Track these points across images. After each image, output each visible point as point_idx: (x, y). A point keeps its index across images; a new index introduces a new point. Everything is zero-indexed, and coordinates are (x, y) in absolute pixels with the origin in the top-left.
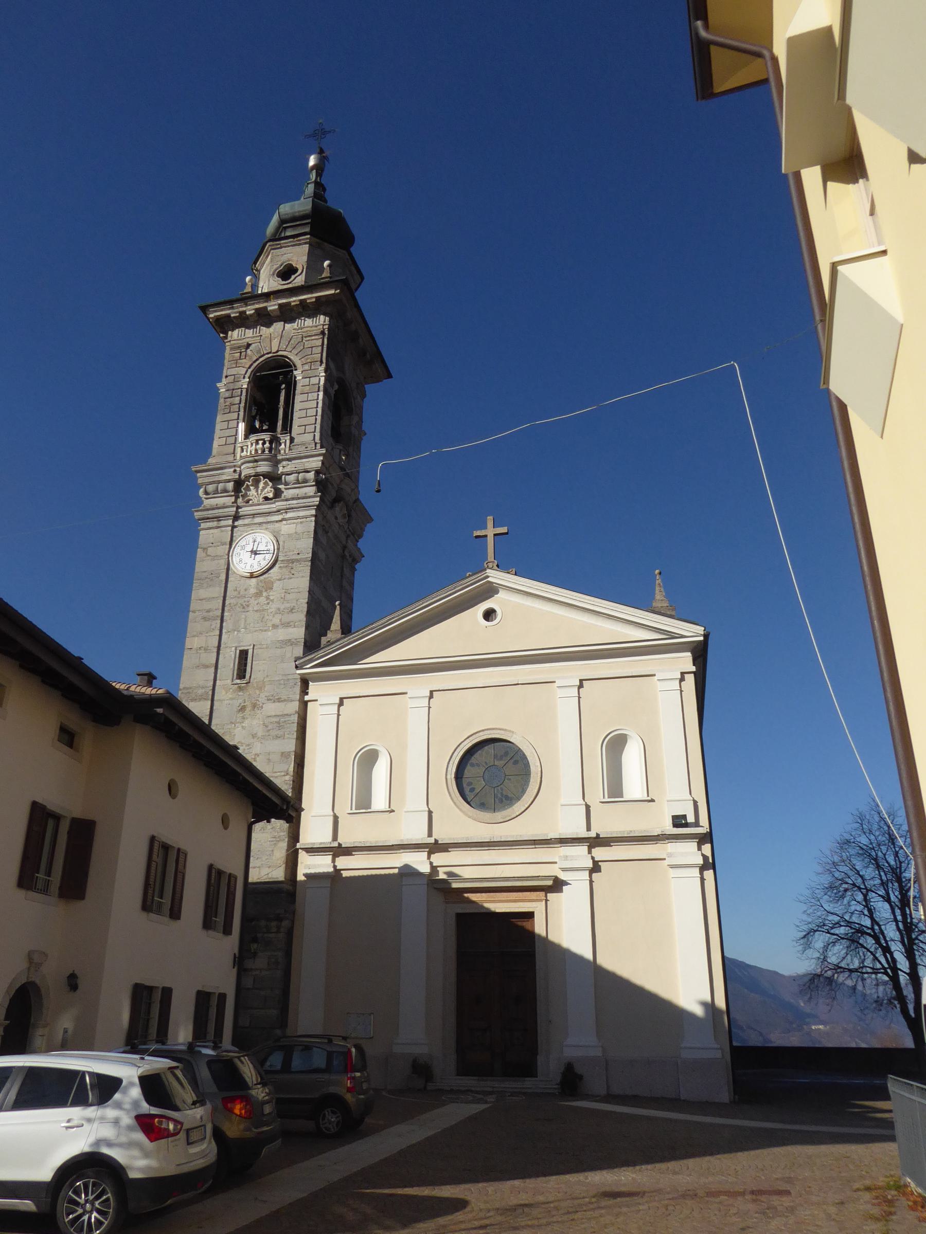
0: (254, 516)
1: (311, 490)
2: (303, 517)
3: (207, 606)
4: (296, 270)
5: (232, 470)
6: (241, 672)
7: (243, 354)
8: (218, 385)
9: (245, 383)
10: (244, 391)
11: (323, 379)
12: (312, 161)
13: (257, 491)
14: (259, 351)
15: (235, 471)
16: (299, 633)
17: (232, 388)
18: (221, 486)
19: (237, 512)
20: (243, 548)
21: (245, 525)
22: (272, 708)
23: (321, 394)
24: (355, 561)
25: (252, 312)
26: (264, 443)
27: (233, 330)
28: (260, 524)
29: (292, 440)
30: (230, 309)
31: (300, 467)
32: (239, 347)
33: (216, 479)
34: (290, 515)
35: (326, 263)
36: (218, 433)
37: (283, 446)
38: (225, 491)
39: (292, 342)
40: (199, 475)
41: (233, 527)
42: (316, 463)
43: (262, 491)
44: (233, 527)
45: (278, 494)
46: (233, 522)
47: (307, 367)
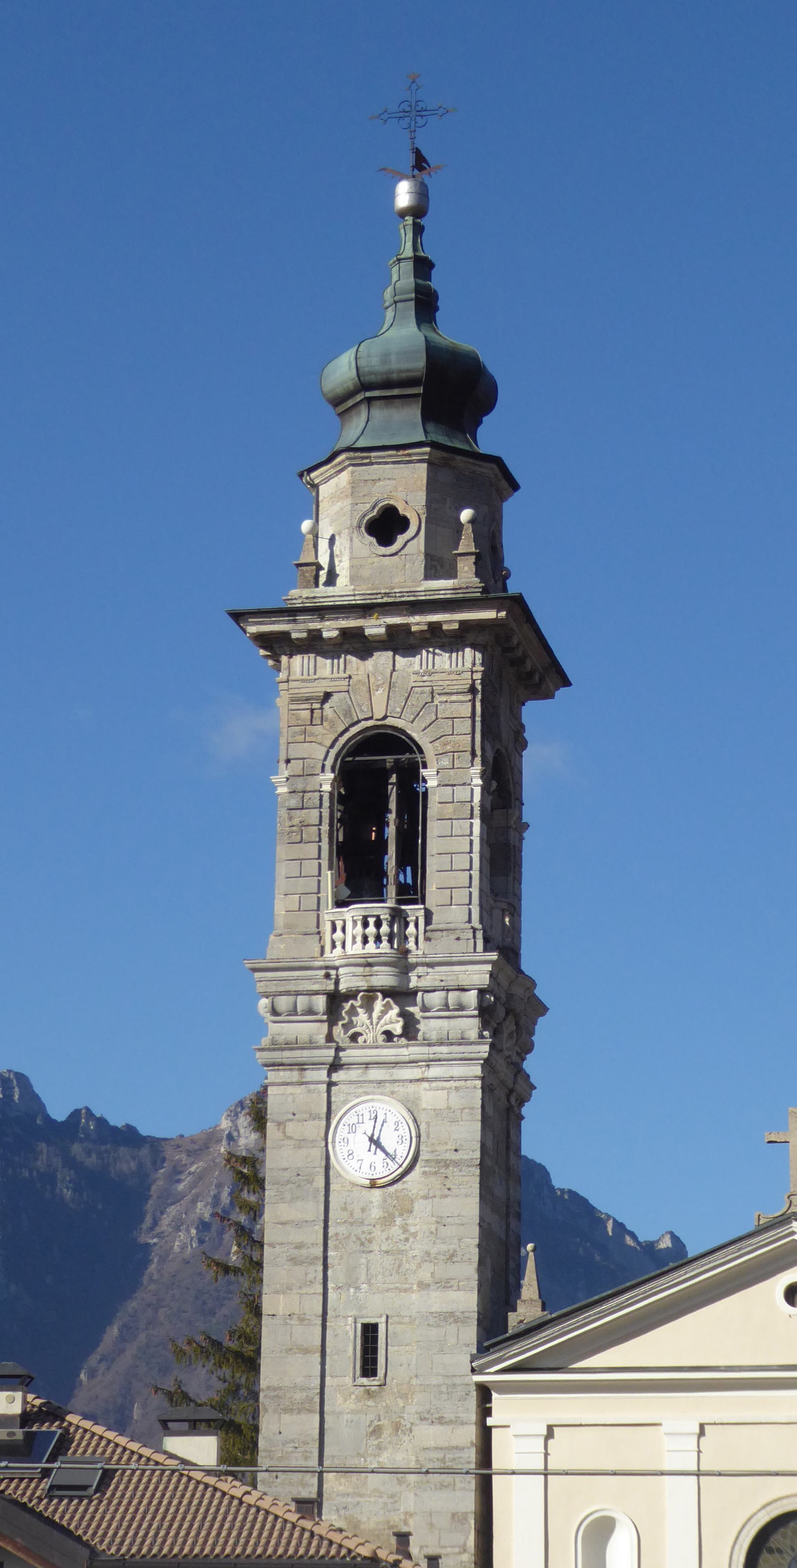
0: (367, 1065)
1: (471, 1026)
2: (460, 1079)
3: (296, 1236)
4: (403, 524)
5: (323, 972)
6: (369, 1367)
7: (317, 713)
8: (274, 779)
9: (326, 781)
10: (326, 798)
11: (478, 791)
12: (404, 195)
13: (370, 1017)
14: (348, 713)
15: (327, 976)
16: (467, 1300)
17: (300, 787)
18: (302, 1002)
19: (336, 1057)
20: (352, 1129)
21: (351, 1082)
22: (430, 1435)
23: (477, 822)
24: (522, 1102)
25: (335, 634)
26: (378, 924)
27: (291, 656)
28: (380, 1082)
29: (428, 915)
30: (289, 622)
31: (451, 982)
32: (307, 699)
33: (292, 987)
34: (435, 1071)
35: (466, 515)
36: (281, 884)
37: (411, 929)
38: (310, 1011)
39: (412, 700)
40: (257, 975)
41: (330, 1085)
42: (479, 975)
43: (380, 1018)
44: (330, 1085)
45: (410, 1031)
46: (329, 1075)
47: (446, 762)
